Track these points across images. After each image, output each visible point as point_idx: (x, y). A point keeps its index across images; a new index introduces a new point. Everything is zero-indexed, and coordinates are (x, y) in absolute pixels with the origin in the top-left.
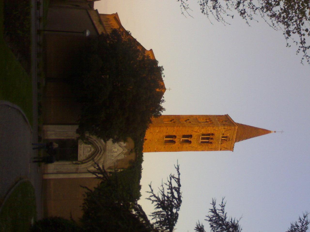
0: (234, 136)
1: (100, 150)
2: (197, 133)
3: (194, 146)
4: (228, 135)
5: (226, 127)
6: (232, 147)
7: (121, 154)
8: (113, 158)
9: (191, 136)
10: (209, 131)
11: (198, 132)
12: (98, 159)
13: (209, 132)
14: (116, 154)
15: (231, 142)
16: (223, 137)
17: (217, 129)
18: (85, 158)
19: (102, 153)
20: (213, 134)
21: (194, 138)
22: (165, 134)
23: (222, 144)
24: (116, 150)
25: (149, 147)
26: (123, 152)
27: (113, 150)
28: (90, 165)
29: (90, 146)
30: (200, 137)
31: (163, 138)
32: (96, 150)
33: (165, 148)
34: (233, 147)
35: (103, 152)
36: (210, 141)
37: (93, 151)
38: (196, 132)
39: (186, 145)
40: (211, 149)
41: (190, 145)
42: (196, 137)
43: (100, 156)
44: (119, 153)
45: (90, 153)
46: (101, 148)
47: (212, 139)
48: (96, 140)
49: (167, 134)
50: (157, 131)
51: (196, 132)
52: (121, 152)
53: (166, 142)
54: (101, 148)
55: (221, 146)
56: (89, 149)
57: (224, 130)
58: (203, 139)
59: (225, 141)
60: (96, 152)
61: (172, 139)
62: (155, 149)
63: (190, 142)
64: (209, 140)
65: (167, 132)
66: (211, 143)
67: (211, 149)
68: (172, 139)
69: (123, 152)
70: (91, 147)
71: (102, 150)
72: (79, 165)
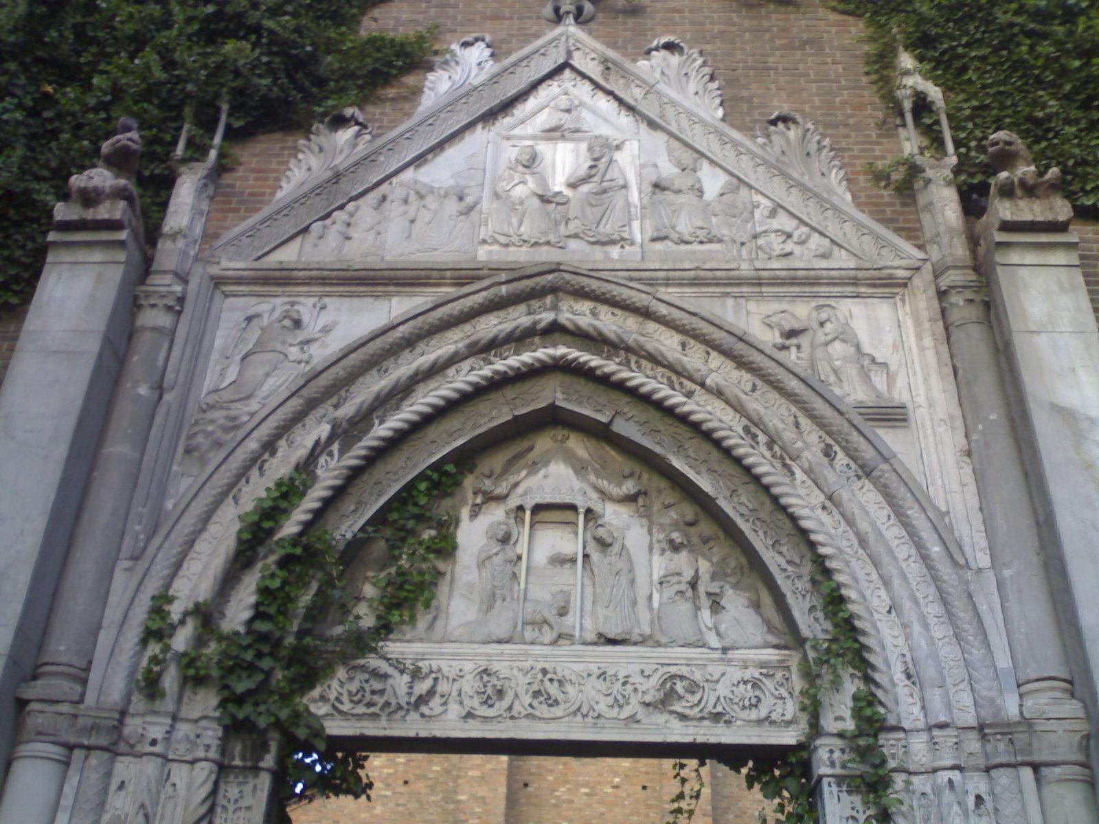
1: (561, 350)
7: (634, 94)
8: (713, 182)
12: (720, 371)
14: (627, 162)
18: (740, 617)
19: (609, 322)
24: (562, 162)
26: (593, 69)
27: (558, 184)
28: (866, 500)
29: (473, 534)
32: (552, 418)
35: (578, 313)
37: (580, 469)
43: (667, 343)
44: (625, 120)
45: (615, 516)
46: (520, 338)
48: (348, 410)
52: (605, 104)
54: (520, 338)
56: (554, 540)
60: (601, 433)
69: (593, 69)
70: (496, 515)
71: (547, 317)
72: (906, 707)
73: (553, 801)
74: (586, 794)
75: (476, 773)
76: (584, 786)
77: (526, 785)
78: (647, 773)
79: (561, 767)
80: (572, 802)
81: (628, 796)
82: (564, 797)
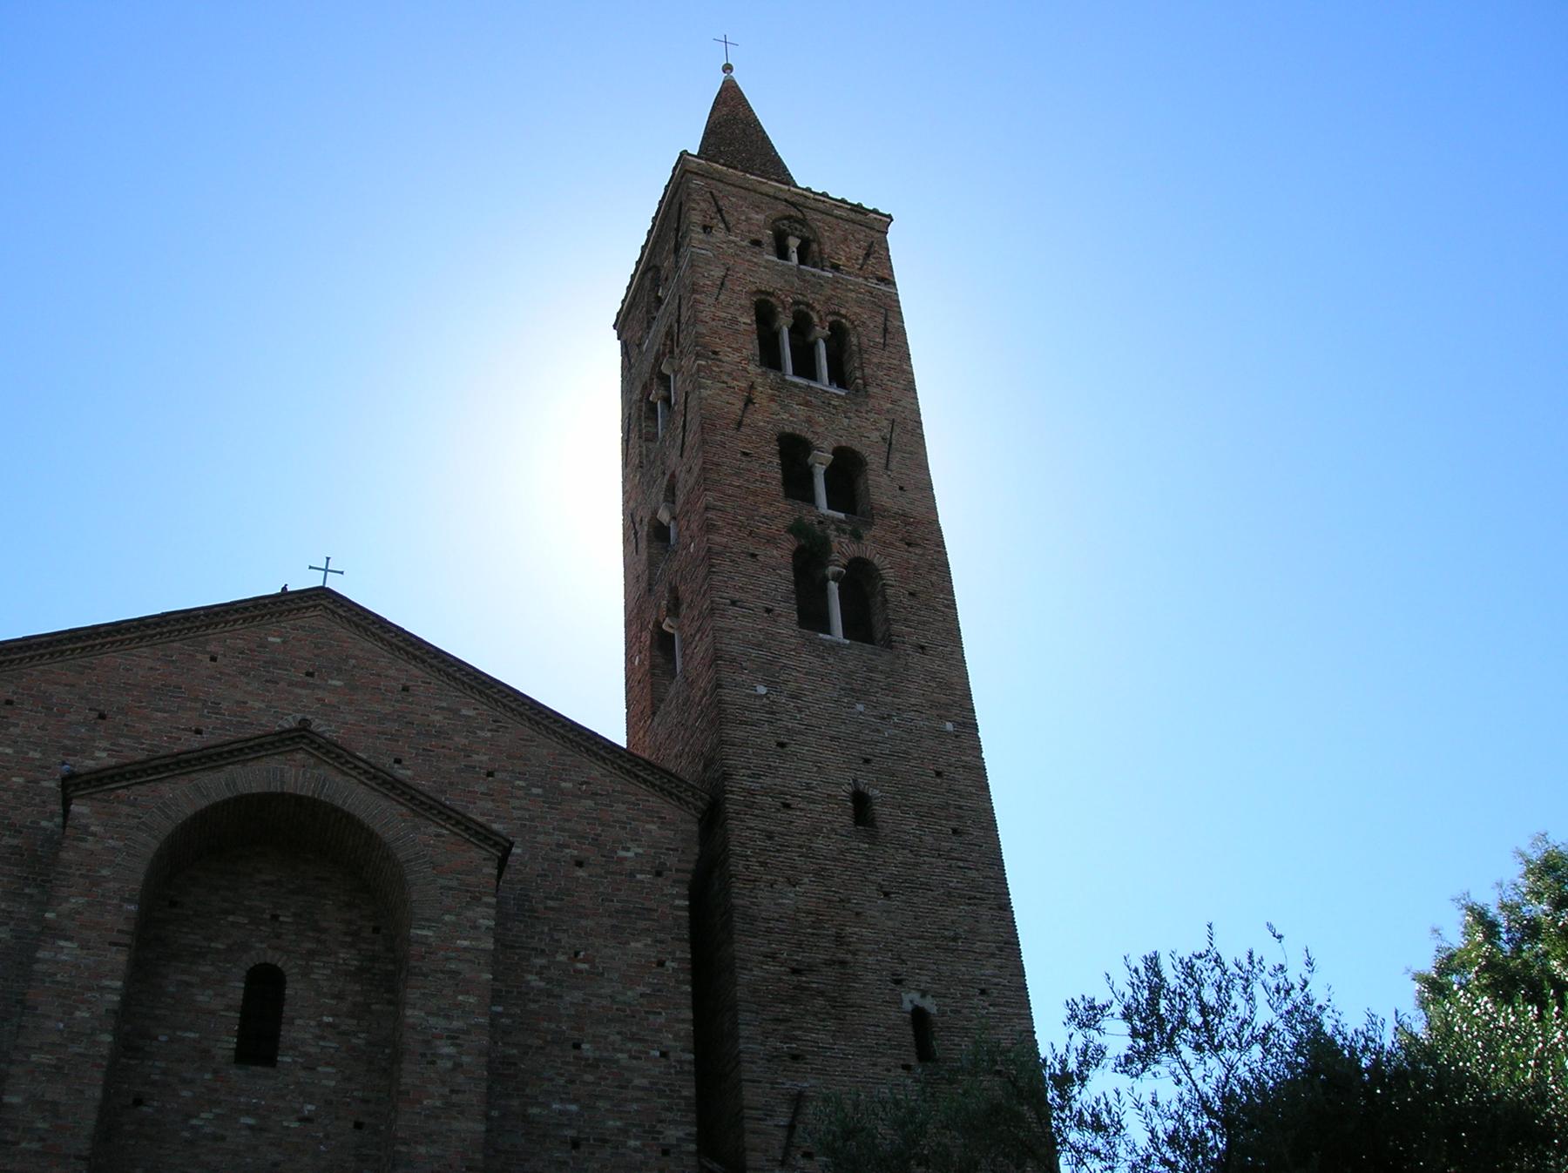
0: (771, 191)
2: (761, 397)
3: (875, 436)
4: (761, 217)
5: (696, 217)
6: (853, 215)
9: (793, 450)
10: (734, 321)
11: (752, 387)
13: (747, 320)
15: (819, 216)
16: (782, 253)
17: (718, 273)
20: (764, 312)
21: (809, 420)
22: (787, 627)
23: (836, 267)
25: (939, 774)
30: (796, 385)
31: (834, 648)
33: (923, 648)
34: (858, 208)
36: (820, 332)
38: (749, 401)
39: (879, 486)
40: (886, 330)
41: (874, 461)
42: (801, 411)
47: (801, 326)
49: (788, 612)
50: (762, 690)
51: (749, 401)
53: (859, 627)
55: (857, 276)
57: (719, 234)
58: (805, 367)
59: (815, 247)
61: (833, 586)
62: (949, 726)
63: (847, 467)
64: (811, 338)
65: (768, 611)
66: (838, 336)
67: (886, 330)
68: (833, 586)
73: (186, 1134)
74: (250, 1127)
75: (48, 1059)
76: (248, 1113)
77: (138, 1102)
78: (365, 1101)
79: (208, 1076)
80: (223, 1138)
81: (327, 1137)
82: (208, 1130)
